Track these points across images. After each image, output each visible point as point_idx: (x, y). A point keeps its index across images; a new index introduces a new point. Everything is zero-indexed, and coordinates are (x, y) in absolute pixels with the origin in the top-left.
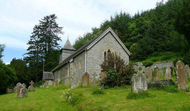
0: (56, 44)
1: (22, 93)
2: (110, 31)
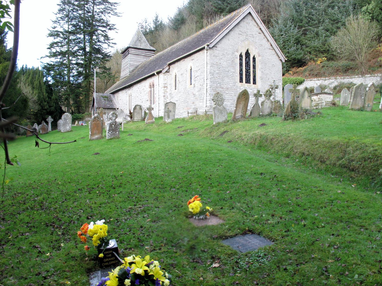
0: (106, 37)
1: (109, 130)
2: (250, 13)
